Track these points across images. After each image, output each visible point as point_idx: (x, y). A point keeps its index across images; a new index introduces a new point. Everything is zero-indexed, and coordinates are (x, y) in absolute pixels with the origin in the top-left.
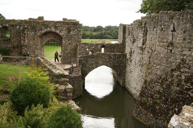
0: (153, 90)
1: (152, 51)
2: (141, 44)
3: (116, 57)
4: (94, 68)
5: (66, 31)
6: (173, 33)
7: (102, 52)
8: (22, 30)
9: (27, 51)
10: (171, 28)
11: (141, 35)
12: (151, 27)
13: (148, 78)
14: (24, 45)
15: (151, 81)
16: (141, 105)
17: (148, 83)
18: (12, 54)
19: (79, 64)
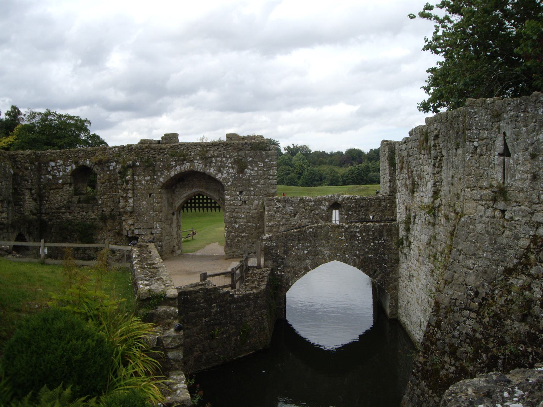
0: (456, 333)
1: (457, 214)
2: (431, 195)
3: (368, 235)
4: (307, 270)
5: (233, 168)
6: (504, 160)
7: (334, 222)
8: (120, 172)
9: (132, 228)
10: (499, 146)
11: (428, 169)
12: (449, 144)
13: (443, 295)
14: (126, 213)
15: (451, 306)
16: (425, 378)
17: (442, 312)
18: (99, 237)
19: (265, 260)
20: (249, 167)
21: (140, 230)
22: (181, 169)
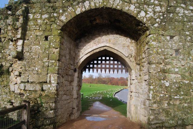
5: (161, 6)
20: (183, 5)
21: (26, 84)
22: (90, 6)
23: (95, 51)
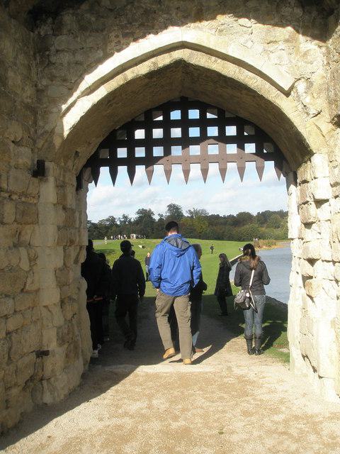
23: (130, 74)
